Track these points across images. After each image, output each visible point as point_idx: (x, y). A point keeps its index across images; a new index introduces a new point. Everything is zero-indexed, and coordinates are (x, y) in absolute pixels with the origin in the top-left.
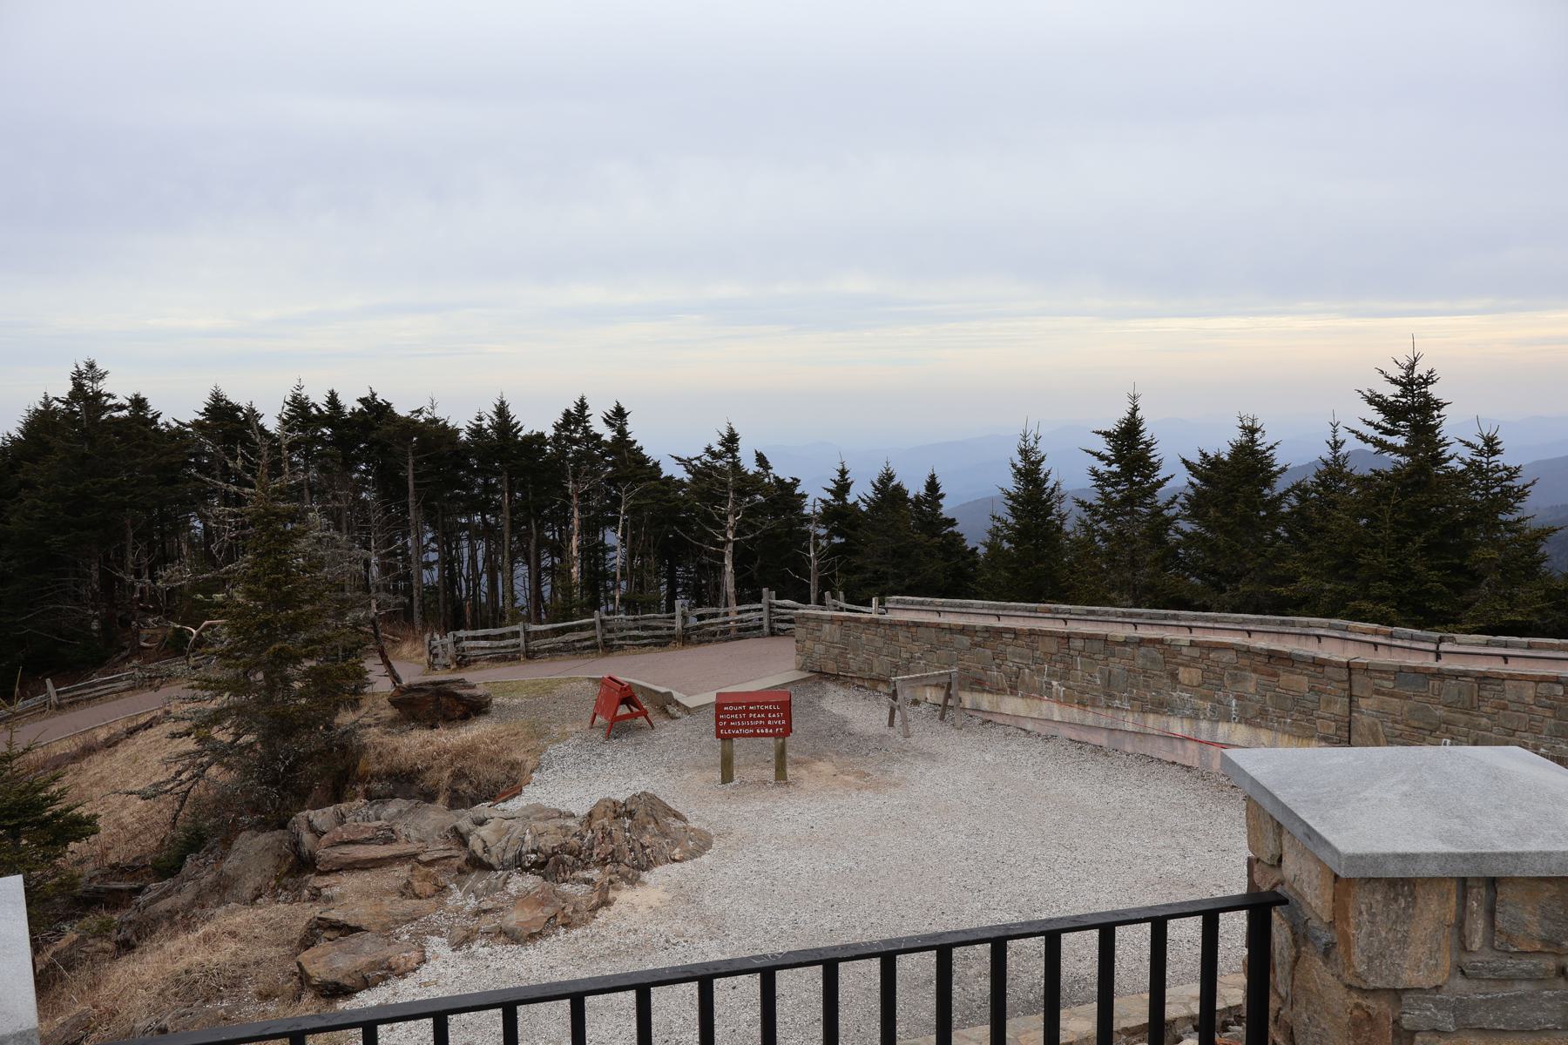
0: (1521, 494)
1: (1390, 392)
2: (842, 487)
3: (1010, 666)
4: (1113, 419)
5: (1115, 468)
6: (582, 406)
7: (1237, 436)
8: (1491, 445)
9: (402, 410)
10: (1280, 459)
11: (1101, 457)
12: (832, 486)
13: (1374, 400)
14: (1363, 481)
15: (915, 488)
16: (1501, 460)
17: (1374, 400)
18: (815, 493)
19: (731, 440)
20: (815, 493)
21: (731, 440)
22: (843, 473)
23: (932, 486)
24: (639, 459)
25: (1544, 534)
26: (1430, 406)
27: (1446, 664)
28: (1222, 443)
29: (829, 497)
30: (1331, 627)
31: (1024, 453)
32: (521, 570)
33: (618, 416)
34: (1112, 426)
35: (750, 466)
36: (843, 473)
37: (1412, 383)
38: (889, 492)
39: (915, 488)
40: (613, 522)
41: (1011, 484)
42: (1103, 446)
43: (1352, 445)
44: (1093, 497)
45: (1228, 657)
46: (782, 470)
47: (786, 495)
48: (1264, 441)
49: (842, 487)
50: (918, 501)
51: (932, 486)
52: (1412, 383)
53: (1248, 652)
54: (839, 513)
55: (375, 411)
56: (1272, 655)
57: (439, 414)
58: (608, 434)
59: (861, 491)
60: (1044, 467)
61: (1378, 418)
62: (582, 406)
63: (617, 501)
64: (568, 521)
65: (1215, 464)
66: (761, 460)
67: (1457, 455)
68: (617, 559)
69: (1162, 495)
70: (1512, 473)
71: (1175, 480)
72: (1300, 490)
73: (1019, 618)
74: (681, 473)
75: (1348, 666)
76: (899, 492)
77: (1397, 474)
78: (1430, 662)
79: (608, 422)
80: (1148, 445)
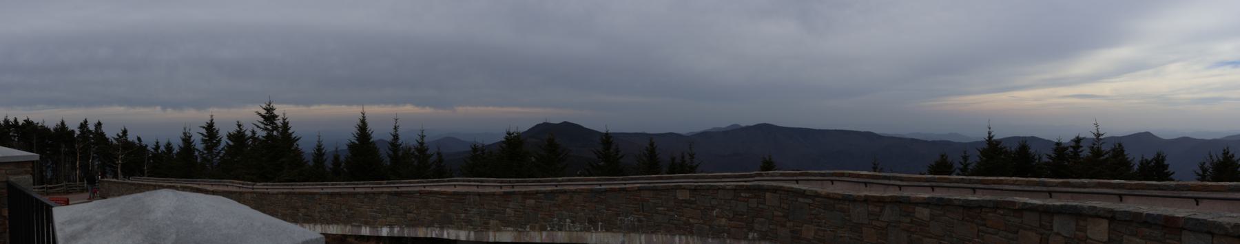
2: (157, 147)
5: (207, 138)
11: (202, 134)
12: (154, 147)
22: (157, 143)
28: (233, 129)
29: (152, 150)
30: (230, 182)
31: (185, 134)
36: (157, 143)
42: (204, 131)
46: (144, 143)
49: (157, 147)
60: (192, 139)
61: (262, 120)
66: (139, 139)
71: (225, 141)
80: (217, 132)
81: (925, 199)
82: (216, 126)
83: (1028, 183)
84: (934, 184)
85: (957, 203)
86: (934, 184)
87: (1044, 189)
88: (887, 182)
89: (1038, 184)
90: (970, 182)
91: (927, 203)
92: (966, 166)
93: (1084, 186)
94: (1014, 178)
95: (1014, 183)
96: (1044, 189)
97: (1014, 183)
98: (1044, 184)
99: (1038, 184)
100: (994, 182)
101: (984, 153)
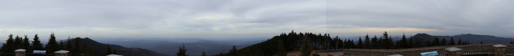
0: (393, 40)
1: (384, 33)
2: (346, 40)
3: (360, 53)
4: (366, 35)
6: (326, 34)
7: (375, 37)
8: (391, 37)
9: (313, 34)
10: (378, 38)
13: (384, 34)
14: (383, 39)
15: (351, 40)
16: (392, 38)
17: (384, 34)
18: (344, 41)
19: (337, 37)
20: (344, 41)
21: (337, 37)
23: (352, 40)
24: (330, 38)
25: (394, 43)
26: (387, 34)
27: (389, 51)
28: (373, 37)
31: (360, 38)
32: (321, 46)
33: (329, 35)
34: (366, 36)
35: (339, 39)
37: (386, 33)
38: (349, 41)
39: (351, 40)
40: (328, 43)
41: (359, 40)
42: (365, 37)
43: (382, 37)
44: (365, 41)
45: (375, 52)
46: (341, 39)
47: (341, 41)
48: (376, 37)
49: (346, 40)
50: (351, 41)
51: (352, 40)
52: (386, 33)
53: (376, 52)
54: (345, 42)
55: (311, 34)
56: (378, 52)
57: (316, 34)
58: (328, 36)
59: (347, 41)
62: (326, 34)
63: (328, 41)
64: (325, 42)
65: (373, 39)
66: (339, 38)
67: (389, 38)
68: (328, 45)
69: (370, 41)
70: (392, 39)
72: (379, 40)
73: (360, 50)
74: (333, 39)
75: (383, 52)
76: (350, 41)
77: (385, 39)
78: (388, 51)
79: (328, 35)
82: (369, 36)
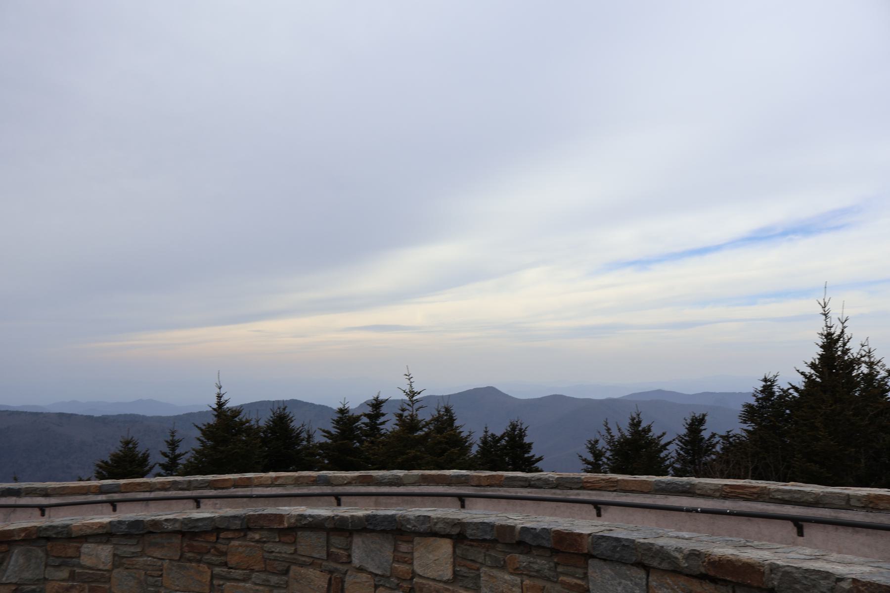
81: (102, 526)
83: (298, 482)
84: (116, 496)
85: (170, 527)
86: (116, 496)
87: (327, 490)
88: (12, 501)
89: (316, 482)
90: (190, 486)
91: (106, 534)
92: (174, 459)
93: (397, 482)
94: (272, 474)
95: (273, 483)
96: (327, 490)
97: (273, 483)
98: (327, 482)
99: (316, 482)
100: (236, 484)
101: (209, 432)
